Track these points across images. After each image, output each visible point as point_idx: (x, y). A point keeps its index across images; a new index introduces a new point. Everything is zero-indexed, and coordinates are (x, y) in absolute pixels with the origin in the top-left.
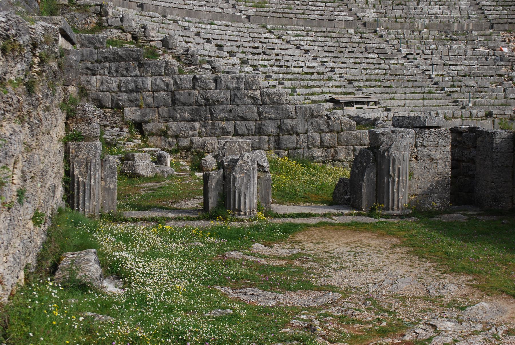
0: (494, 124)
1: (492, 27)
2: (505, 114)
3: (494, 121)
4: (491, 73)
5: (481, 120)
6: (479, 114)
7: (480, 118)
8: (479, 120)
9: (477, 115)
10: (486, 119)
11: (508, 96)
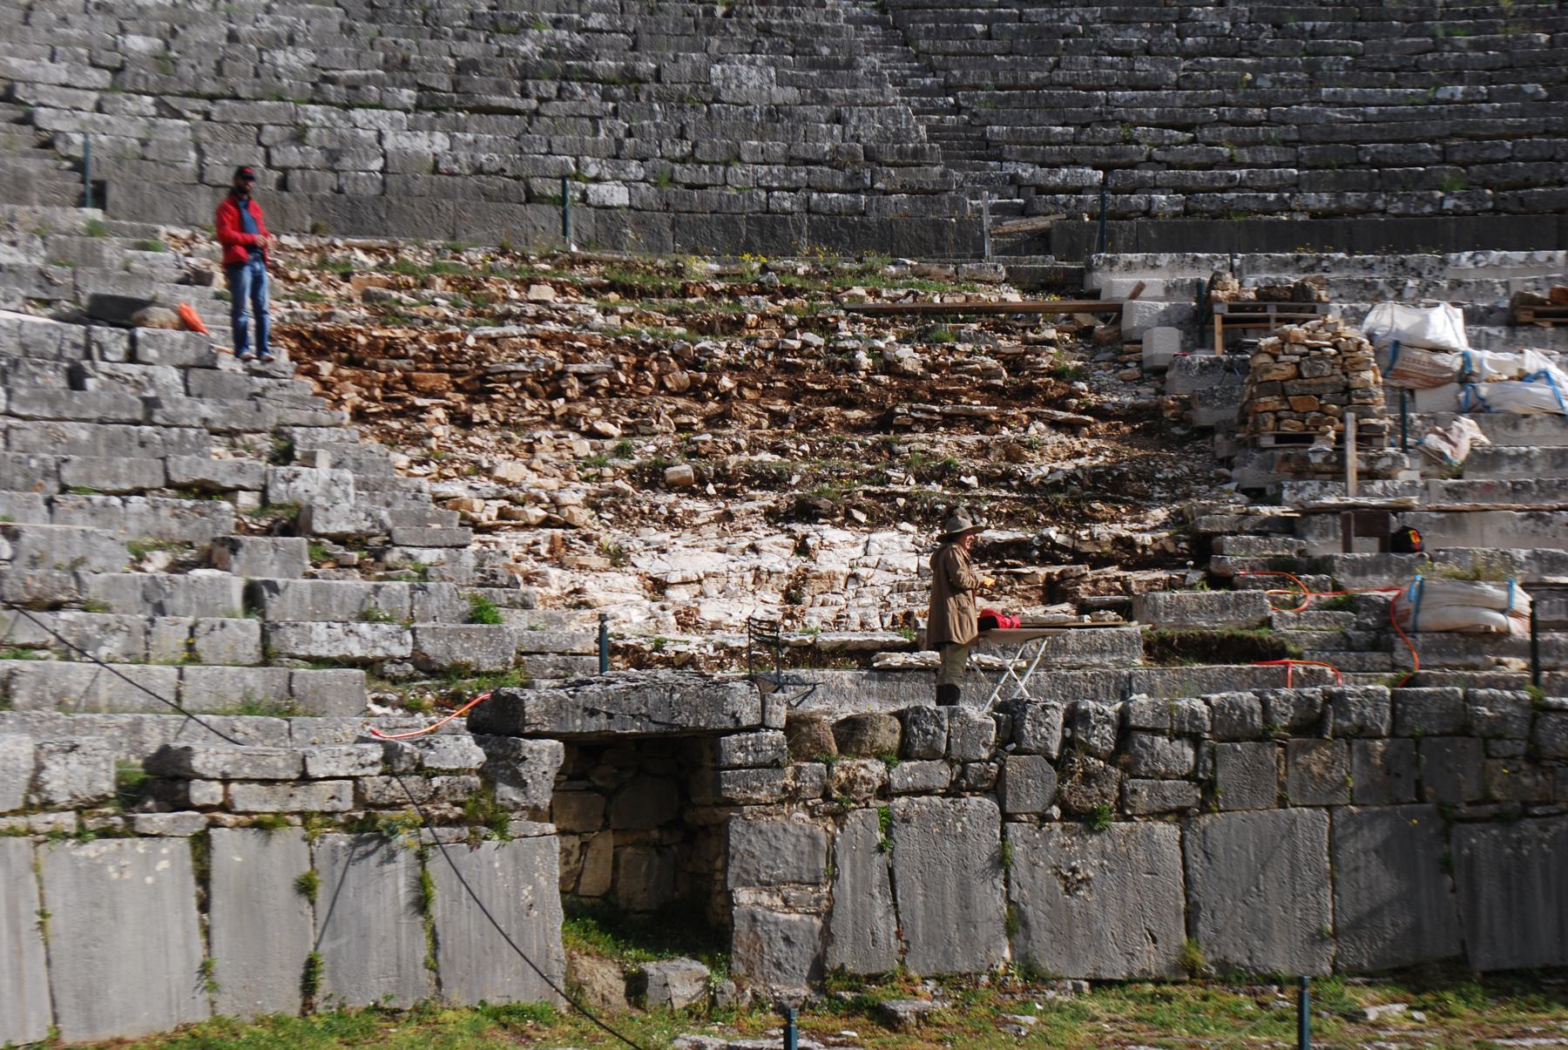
0: (203, 878)
1: (98, 195)
2: (305, 779)
3: (201, 844)
4: (129, 468)
5: (81, 835)
6: (62, 779)
7: (68, 820)
8: (58, 835)
9: (35, 785)
10: (130, 831)
11: (290, 640)
